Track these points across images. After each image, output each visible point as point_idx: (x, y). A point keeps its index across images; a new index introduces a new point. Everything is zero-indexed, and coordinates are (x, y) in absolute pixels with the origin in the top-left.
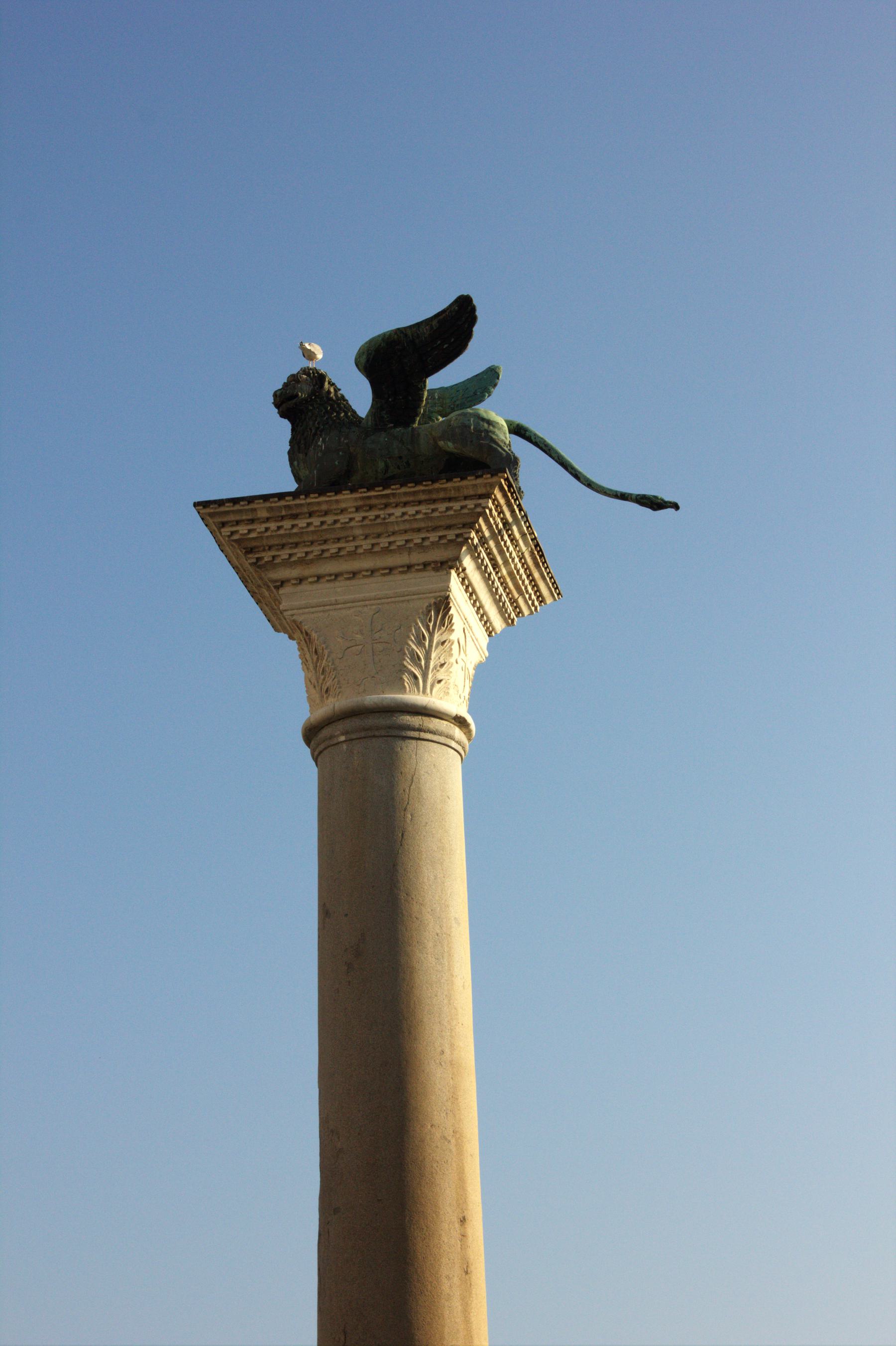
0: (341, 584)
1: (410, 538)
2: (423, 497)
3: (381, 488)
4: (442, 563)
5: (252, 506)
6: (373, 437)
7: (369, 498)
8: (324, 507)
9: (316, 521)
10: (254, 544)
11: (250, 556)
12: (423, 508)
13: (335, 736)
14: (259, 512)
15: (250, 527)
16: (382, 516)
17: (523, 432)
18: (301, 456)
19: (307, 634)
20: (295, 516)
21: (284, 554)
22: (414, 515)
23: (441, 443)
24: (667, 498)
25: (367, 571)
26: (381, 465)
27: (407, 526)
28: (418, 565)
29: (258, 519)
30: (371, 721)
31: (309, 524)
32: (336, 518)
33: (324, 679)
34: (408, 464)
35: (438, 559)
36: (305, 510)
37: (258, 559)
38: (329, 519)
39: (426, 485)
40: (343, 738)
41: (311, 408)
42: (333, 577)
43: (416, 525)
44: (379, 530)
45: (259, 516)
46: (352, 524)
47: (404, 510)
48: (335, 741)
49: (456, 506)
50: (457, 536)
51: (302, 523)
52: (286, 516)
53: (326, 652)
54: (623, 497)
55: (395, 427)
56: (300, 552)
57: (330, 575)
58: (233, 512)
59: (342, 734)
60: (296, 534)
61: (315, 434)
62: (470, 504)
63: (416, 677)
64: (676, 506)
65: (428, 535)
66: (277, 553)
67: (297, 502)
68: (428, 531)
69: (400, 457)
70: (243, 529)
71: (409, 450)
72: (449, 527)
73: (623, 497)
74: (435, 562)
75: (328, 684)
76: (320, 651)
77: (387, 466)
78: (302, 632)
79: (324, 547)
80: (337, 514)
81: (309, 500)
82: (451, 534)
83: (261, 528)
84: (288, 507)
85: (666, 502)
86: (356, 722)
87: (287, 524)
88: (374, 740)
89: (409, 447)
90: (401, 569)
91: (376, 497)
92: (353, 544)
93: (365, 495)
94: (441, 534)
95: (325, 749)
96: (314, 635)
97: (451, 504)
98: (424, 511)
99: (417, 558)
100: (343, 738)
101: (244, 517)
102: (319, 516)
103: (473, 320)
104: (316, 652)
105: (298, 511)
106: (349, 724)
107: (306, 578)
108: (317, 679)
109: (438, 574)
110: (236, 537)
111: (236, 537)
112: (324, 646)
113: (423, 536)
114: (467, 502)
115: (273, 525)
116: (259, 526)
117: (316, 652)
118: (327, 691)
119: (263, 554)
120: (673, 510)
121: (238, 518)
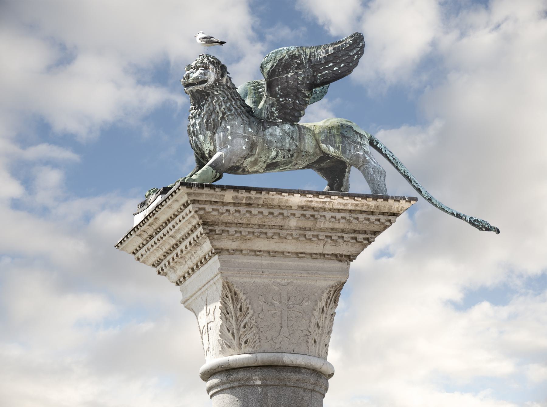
0: (266, 261)
1: (330, 234)
2: (350, 207)
3: (323, 197)
4: (345, 255)
5: (223, 193)
6: (270, 130)
7: (311, 201)
8: (276, 202)
9: (266, 211)
10: (212, 218)
11: (206, 227)
12: (347, 215)
13: (252, 380)
14: (225, 197)
15: (215, 207)
16: (316, 216)
17: (375, 144)
18: (209, 133)
19: (235, 294)
20: (249, 205)
21: (232, 230)
22: (339, 220)
23: (324, 146)
24: (493, 224)
25: (289, 252)
26: (274, 154)
27: (331, 225)
28: (328, 254)
29: (223, 202)
30: (285, 374)
31: (259, 212)
32: (281, 211)
33: (245, 332)
34: (292, 156)
35: (344, 253)
36: (261, 202)
37: (211, 231)
38: (276, 212)
39: (357, 200)
40: (259, 382)
41: (216, 93)
42: (261, 253)
43: (337, 226)
44: (309, 224)
45: (224, 201)
46: (292, 217)
47: (333, 214)
48: (251, 383)
49: (373, 218)
50: (365, 239)
51: (255, 211)
52: (245, 203)
53: (251, 312)
54: (458, 216)
55: (283, 123)
56: (244, 231)
57: (260, 251)
58: (207, 194)
59: (260, 379)
60: (247, 218)
61: (222, 118)
62: (383, 219)
63: (315, 342)
64: (498, 231)
65: (343, 235)
66: (227, 229)
67: (259, 195)
68: (343, 231)
69: (289, 151)
70: (208, 208)
71: (297, 146)
72: (359, 232)
73: (458, 216)
74: (341, 256)
75: (248, 336)
76: (244, 309)
77: (277, 155)
78: (231, 291)
79: (264, 230)
80: (282, 209)
81: (267, 196)
82: (360, 237)
83: (223, 209)
84: (250, 198)
85: (491, 227)
86: (273, 373)
87: (243, 210)
88: (284, 388)
89: (297, 143)
90: (314, 256)
91: (317, 202)
92: (284, 232)
93: (310, 199)
94: (353, 235)
95: (239, 386)
96: (241, 296)
97: (369, 216)
98: (348, 218)
99: (329, 249)
100: (259, 382)
101: (213, 200)
102: (268, 208)
103: (361, 52)
104: (241, 310)
105: (255, 201)
106: (266, 373)
107: (241, 251)
108: (238, 330)
109: (340, 263)
110: (202, 212)
111: (202, 212)
112: (250, 306)
113: (340, 234)
114: (381, 217)
115: (232, 209)
116: (222, 208)
117: (241, 310)
118: (246, 342)
119: (216, 228)
120: (493, 233)
121: (208, 199)
